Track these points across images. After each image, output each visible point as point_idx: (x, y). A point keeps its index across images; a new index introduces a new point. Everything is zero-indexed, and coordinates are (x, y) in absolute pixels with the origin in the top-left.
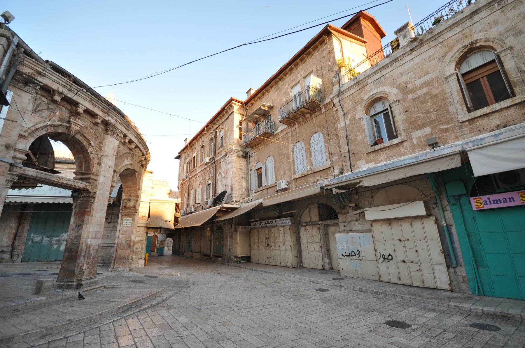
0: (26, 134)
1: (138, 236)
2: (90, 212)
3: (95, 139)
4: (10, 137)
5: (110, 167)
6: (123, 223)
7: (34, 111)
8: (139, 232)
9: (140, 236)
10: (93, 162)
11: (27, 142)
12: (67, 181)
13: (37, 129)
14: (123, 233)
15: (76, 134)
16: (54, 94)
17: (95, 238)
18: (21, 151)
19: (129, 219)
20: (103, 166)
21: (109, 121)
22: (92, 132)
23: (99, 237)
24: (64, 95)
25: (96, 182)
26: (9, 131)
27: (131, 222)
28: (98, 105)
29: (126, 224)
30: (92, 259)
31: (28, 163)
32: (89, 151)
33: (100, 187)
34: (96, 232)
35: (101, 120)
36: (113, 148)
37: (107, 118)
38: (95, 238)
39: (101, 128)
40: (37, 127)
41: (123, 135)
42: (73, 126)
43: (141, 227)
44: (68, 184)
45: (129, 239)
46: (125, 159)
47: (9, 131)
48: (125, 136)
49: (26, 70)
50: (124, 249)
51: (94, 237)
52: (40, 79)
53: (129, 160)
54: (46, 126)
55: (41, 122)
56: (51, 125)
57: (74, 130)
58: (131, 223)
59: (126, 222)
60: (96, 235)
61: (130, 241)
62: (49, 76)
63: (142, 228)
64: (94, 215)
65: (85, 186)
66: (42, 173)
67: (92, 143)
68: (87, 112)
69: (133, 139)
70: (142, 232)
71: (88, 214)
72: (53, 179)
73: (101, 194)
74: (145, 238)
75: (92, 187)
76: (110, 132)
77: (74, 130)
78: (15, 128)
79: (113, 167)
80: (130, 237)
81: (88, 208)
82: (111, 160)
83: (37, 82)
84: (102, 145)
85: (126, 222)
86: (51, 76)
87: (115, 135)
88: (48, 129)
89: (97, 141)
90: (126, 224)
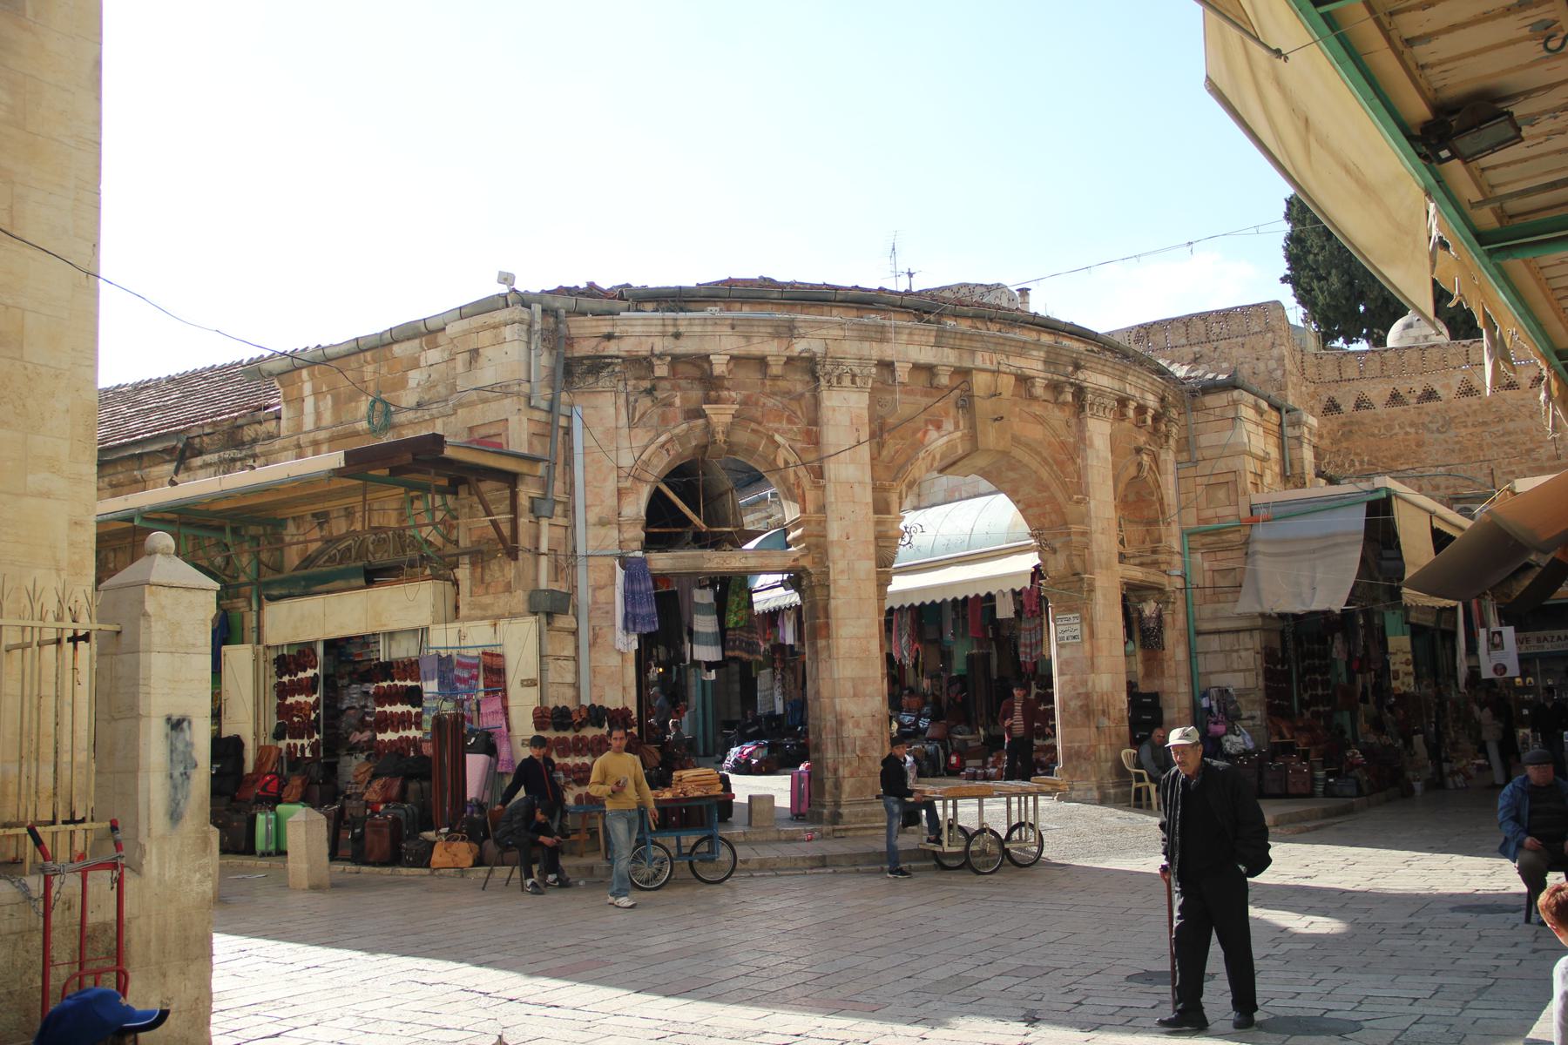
0: (628, 484)
1: (1234, 671)
2: (827, 625)
3: (790, 421)
4: (603, 501)
5: (856, 486)
6: (1059, 635)
7: (632, 425)
8: (1235, 655)
9: (1241, 671)
10: (799, 487)
11: (638, 499)
12: (743, 560)
13: (647, 463)
14: (1064, 667)
15: (727, 434)
16: (651, 367)
17: (855, 695)
18: (634, 522)
19: (1071, 616)
20: (830, 488)
21: (804, 355)
22: (775, 405)
23: (868, 692)
24: (669, 355)
25: (822, 539)
26: (597, 490)
27: (1078, 626)
28: (756, 329)
29: (1066, 635)
30: (858, 752)
31: (653, 542)
32: (781, 464)
33: (835, 552)
34: (853, 679)
35: (782, 363)
36: (848, 424)
37: (799, 346)
38: (855, 695)
39: (797, 382)
40: (644, 457)
41: (876, 365)
42: (714, 419)
43: (1238, 631)
44: (747, 568)
45: (1082, 690)
46: (926, 433)
47: (597, 490)
48: (887, 366)
49: (584, 348)
50: (1077, 726)
51: (851, 693)
52: (612, 348)
53: (948, 425)
54: (662, 446)
55: (652, 441)
56: (670, 440)
57: (720, 429)
58: (1077, 633)
59: (1064, 628)
60: (854, 687)
61: (1087, 696)
62: (627, 332)
63: (1241, 635)
64: (834, 636)
65: (794, 561)
66: (682, 557)
67: (777, 438)
68: (735, 359)
69: (926, 355)
70: (1243, 654)
71: (824, 633)
72: (709, 565)
73: (842, 572)
74: (1261, 678)
75: (813, 558)
76: (823, 382)
77: (720, 429)
78: (605, 480)
79: (868, 479)
80: (1084, 683)
81: (818, 618)
82: (853, 461)
83: (609, 360)
84: (814, 428)
85: (1064, 628)
86: (629, 329)
87: (847, 381)
88: (668, 450)
89: (795, 423)
90: (1066, 635)
